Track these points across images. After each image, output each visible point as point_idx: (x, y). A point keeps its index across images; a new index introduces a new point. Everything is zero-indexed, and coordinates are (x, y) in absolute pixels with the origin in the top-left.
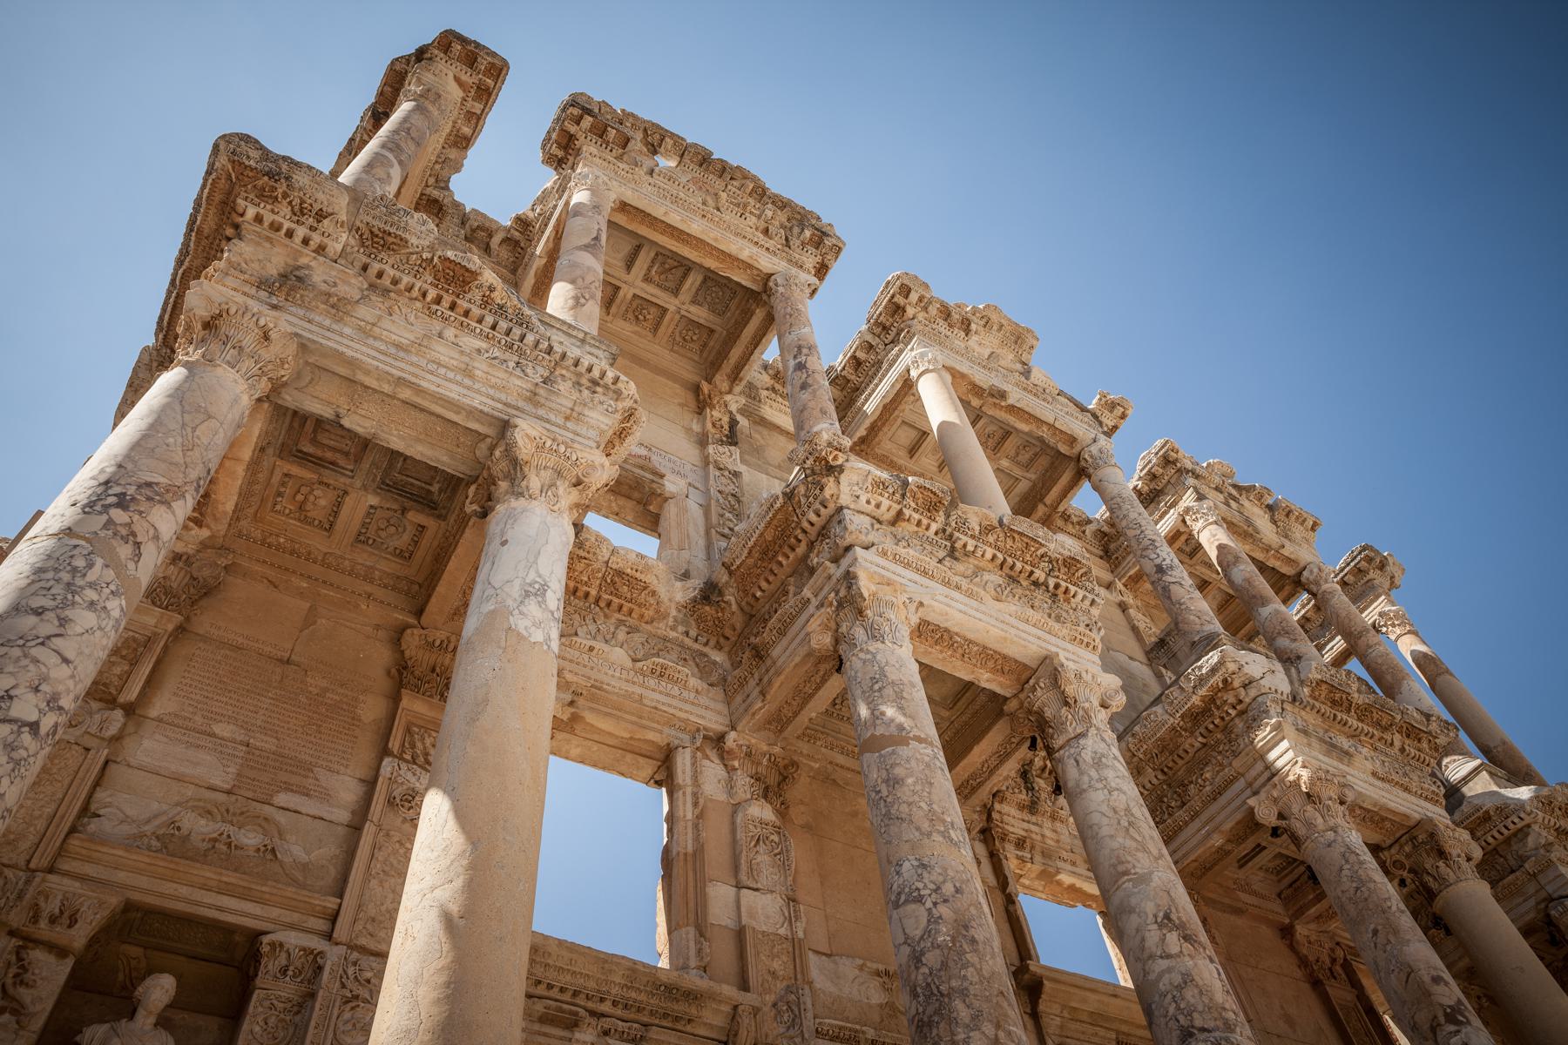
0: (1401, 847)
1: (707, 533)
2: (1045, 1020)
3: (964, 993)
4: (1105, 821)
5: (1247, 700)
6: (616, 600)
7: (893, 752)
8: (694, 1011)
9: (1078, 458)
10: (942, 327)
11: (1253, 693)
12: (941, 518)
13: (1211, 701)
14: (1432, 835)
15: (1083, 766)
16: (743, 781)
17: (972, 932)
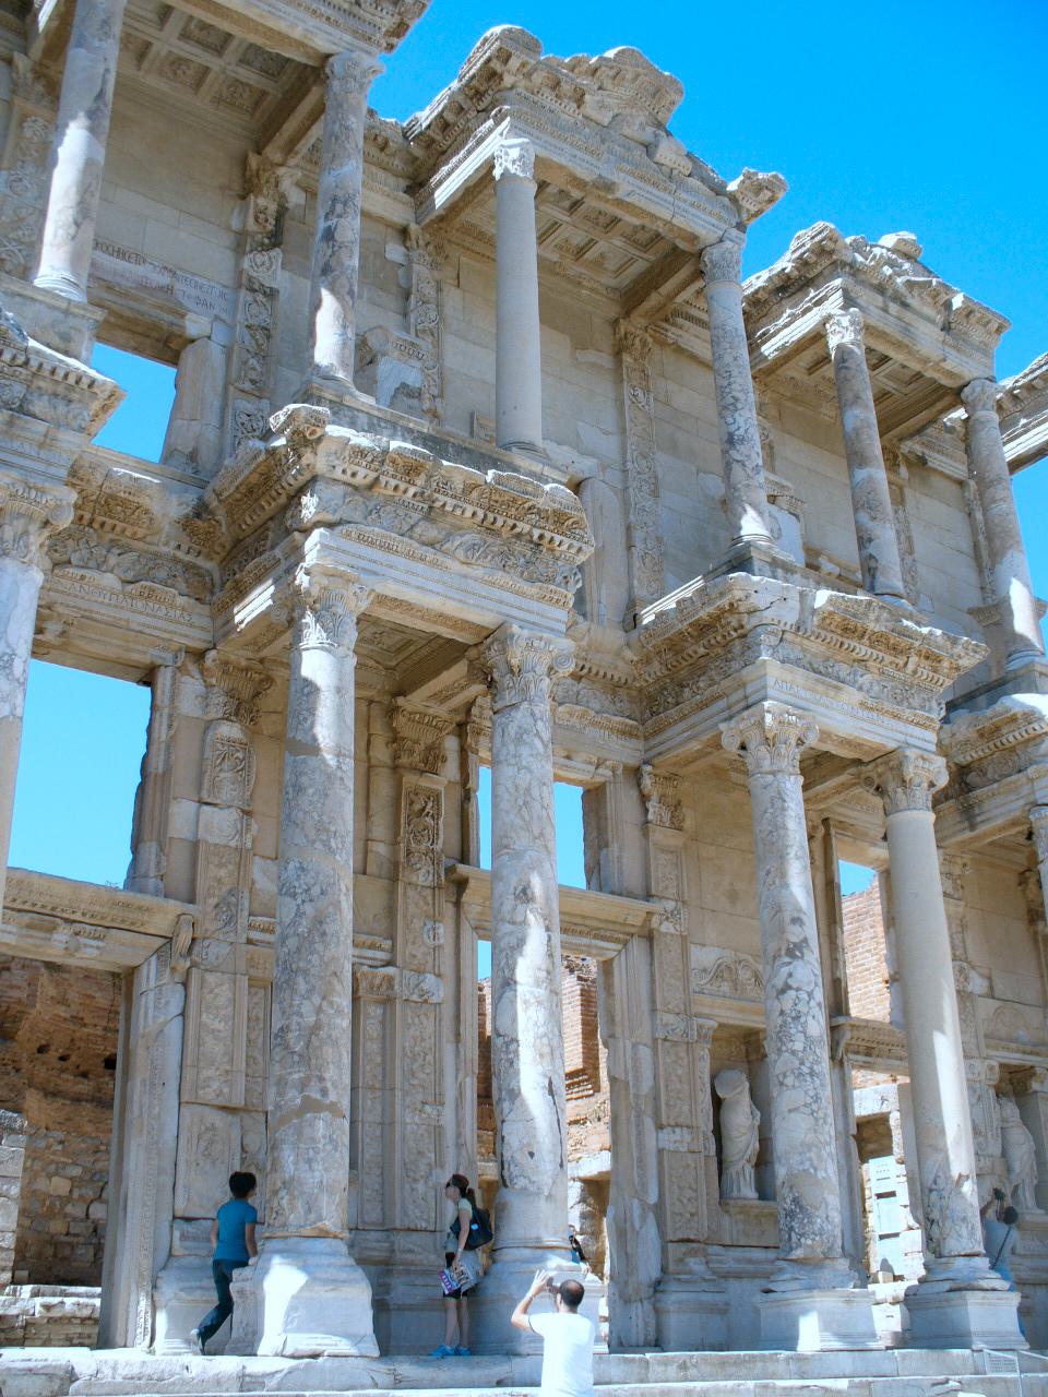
0: (877, 766)
1: (225, 389)
2: (466, 908)
3: (306, 973)
4: (506, 796)
5: (748, 627)
6: (110, 522)
7: (304, 761)
8: (146, 918)
9: (700, 254)
10: (547, 98)
11: (754, 621)
12: (420, 481)
13: (718, 617)
14: (901, 764)
15: (506, 738)
16: (218, 699)
17: (325, 926)
